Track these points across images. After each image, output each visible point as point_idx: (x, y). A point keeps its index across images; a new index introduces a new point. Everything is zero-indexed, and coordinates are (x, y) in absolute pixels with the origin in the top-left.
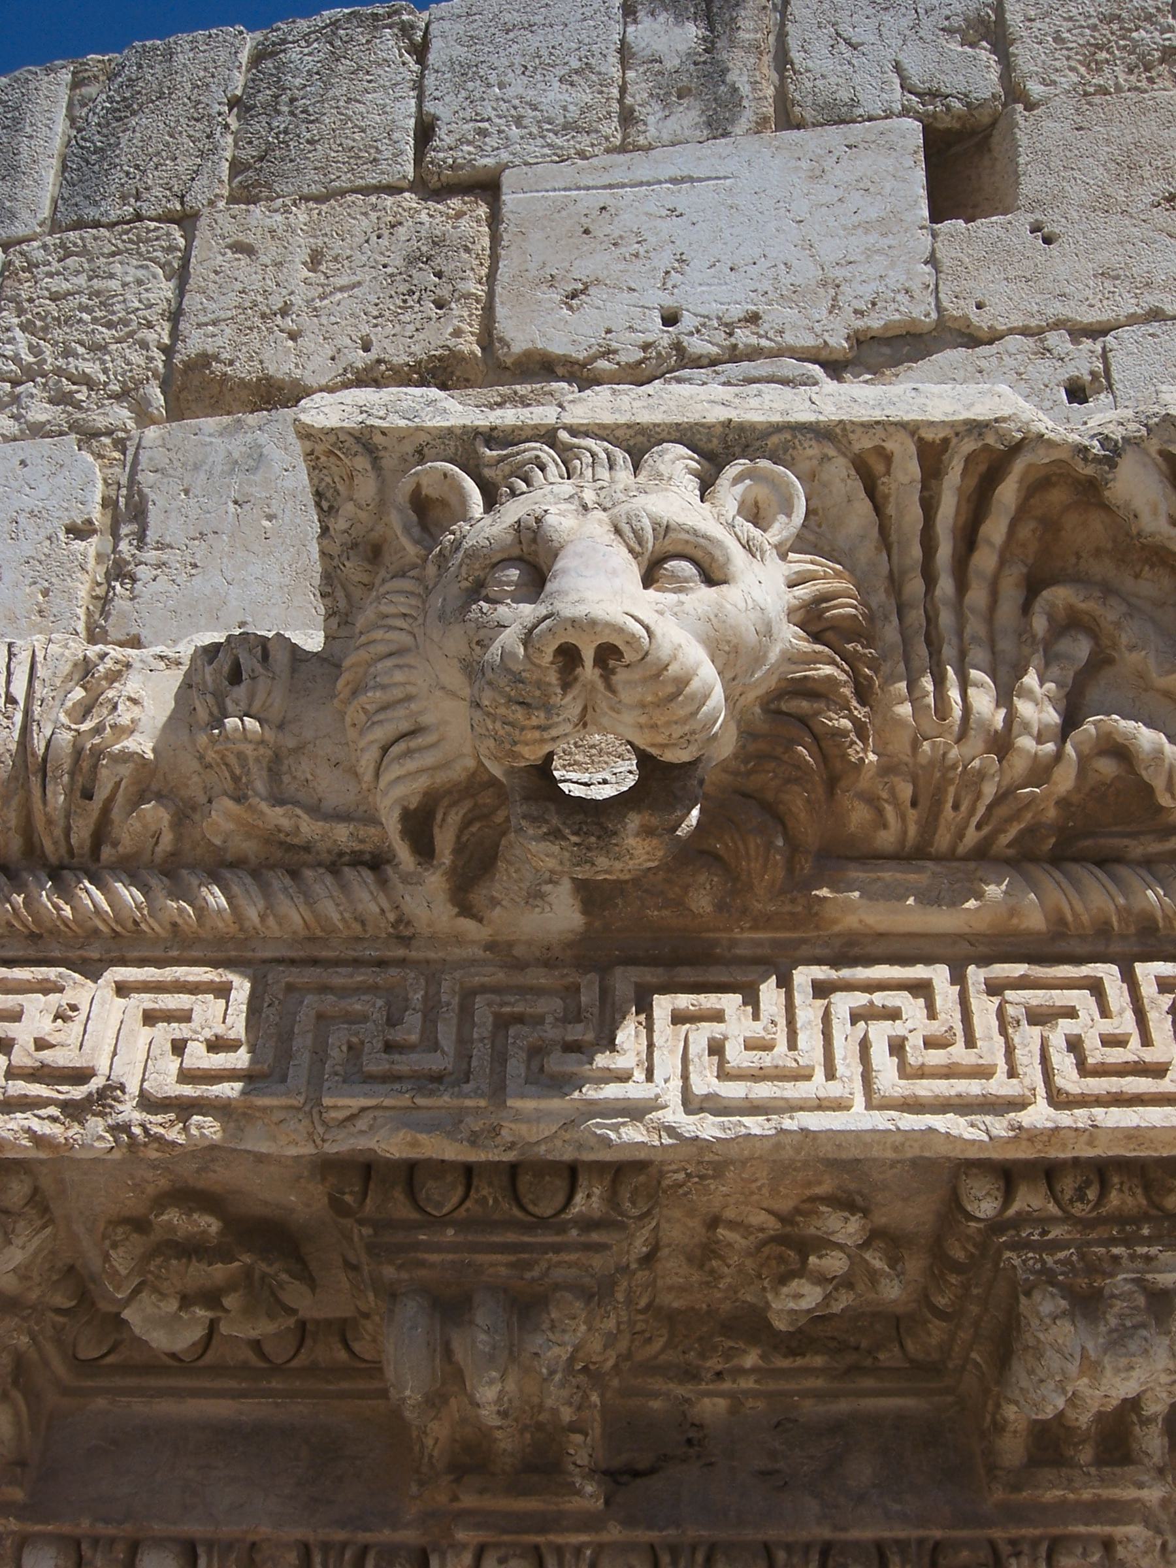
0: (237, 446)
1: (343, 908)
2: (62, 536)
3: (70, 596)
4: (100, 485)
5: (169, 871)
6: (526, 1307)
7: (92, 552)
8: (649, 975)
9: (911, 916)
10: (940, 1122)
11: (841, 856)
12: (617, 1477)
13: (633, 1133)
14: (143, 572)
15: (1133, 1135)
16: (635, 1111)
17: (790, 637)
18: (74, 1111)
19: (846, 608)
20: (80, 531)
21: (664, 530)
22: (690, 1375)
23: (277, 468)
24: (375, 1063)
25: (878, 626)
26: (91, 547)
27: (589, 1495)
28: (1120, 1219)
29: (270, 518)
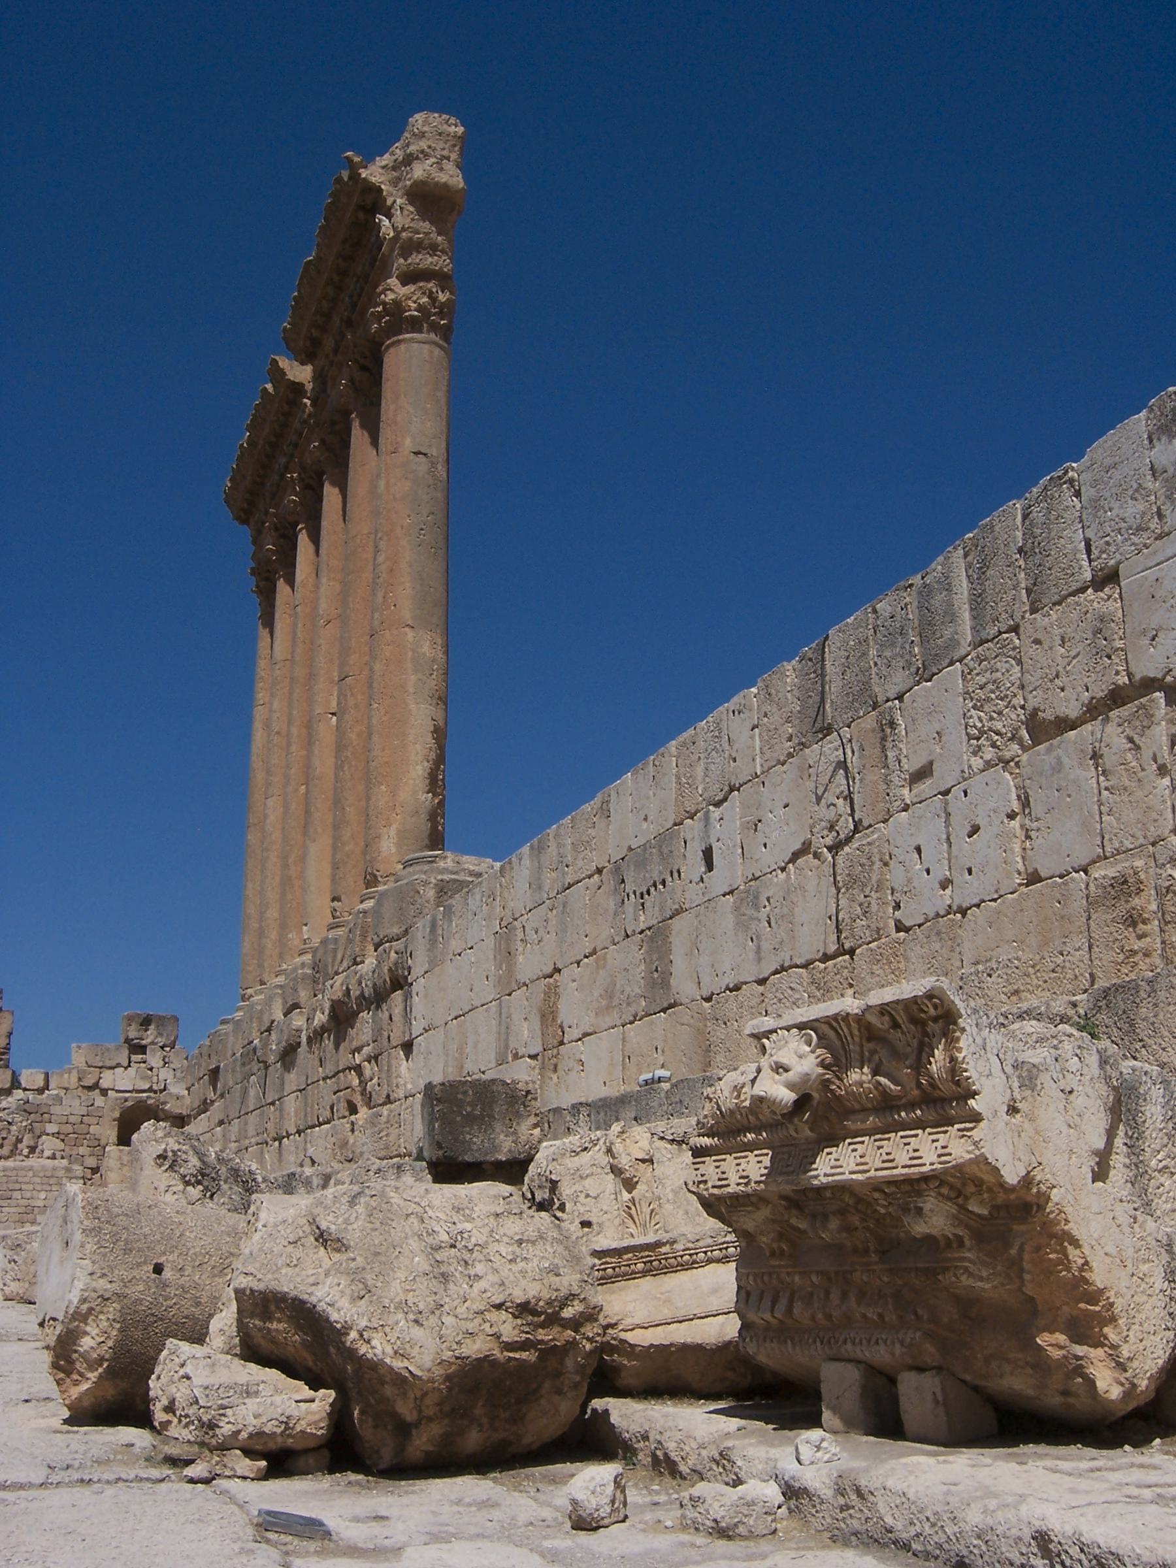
0: (1050, 759)
1: (782, 1134)
2: (1006, 821)
3: (1012, 849)
4: (1014, 789)
5: (757, 1130)
6: (825, 1217)
7: (1018, 825)
8: (826, 1144)
9: (859, 1125)
10: (854, 1176)
11: (849, 1113)
12: (883, 1253)
13: (815, 1182)
14: (1033, 834)
15: (883, 1177)
16: (816, 1177)
17: (820, 1070)
18: (746, 1184)
19: (828, 1061)
20: (1012, 816)
21: (776, 1063)
22: (897, 1227)
23: (1067, 767)
24: (785, 1170)
25: (838, 1063)
26: (1015, 824)
27: (874, 1257)
28: (907, 1192)
29: (1069, 796)
